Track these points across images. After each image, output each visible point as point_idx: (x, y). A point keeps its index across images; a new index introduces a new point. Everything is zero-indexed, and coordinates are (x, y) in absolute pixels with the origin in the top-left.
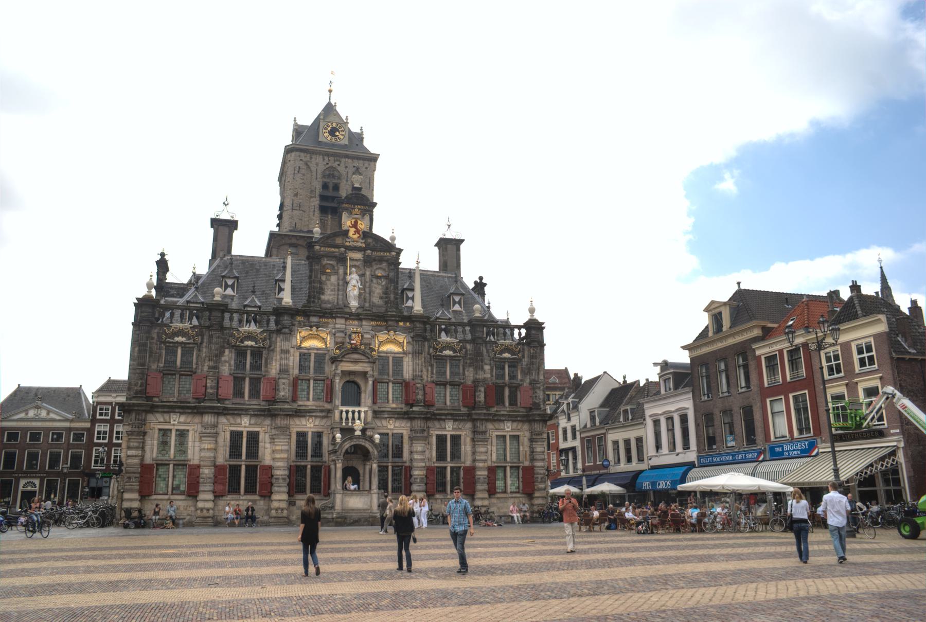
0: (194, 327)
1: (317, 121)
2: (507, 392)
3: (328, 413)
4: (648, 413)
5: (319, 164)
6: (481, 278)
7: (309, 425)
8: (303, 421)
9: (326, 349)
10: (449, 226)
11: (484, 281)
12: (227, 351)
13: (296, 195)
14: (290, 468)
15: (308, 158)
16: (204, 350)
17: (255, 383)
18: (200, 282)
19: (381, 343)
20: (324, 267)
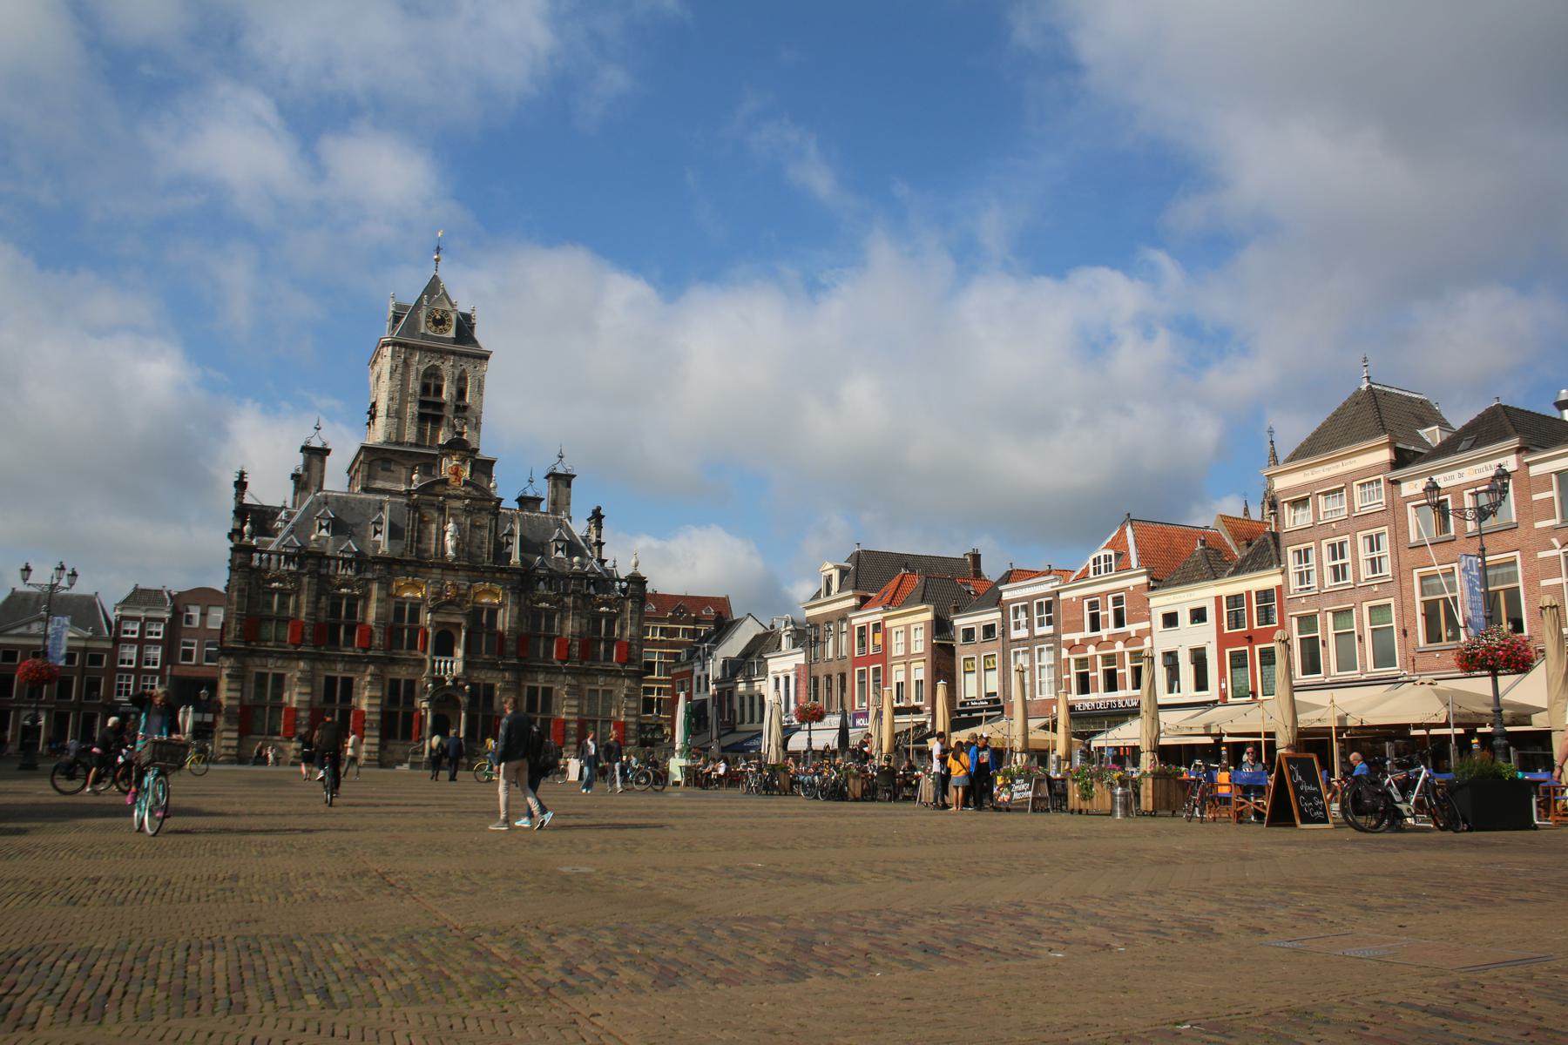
0: (291, 573)
1: (419, 303)
2: (602, 647)
3: (422, 662)
4: (771, 669)
5: (419, 363)
6: (599, 509)
7: (402, 673)
8: (397, 669)
9: (424, 599)
12: (323, 599)
13: (391, 399)
14: (382, 713)
16: (304, 599)
17: (350, 631)
18: (294, 520)
19: (476, 594)
20: (422, 516)
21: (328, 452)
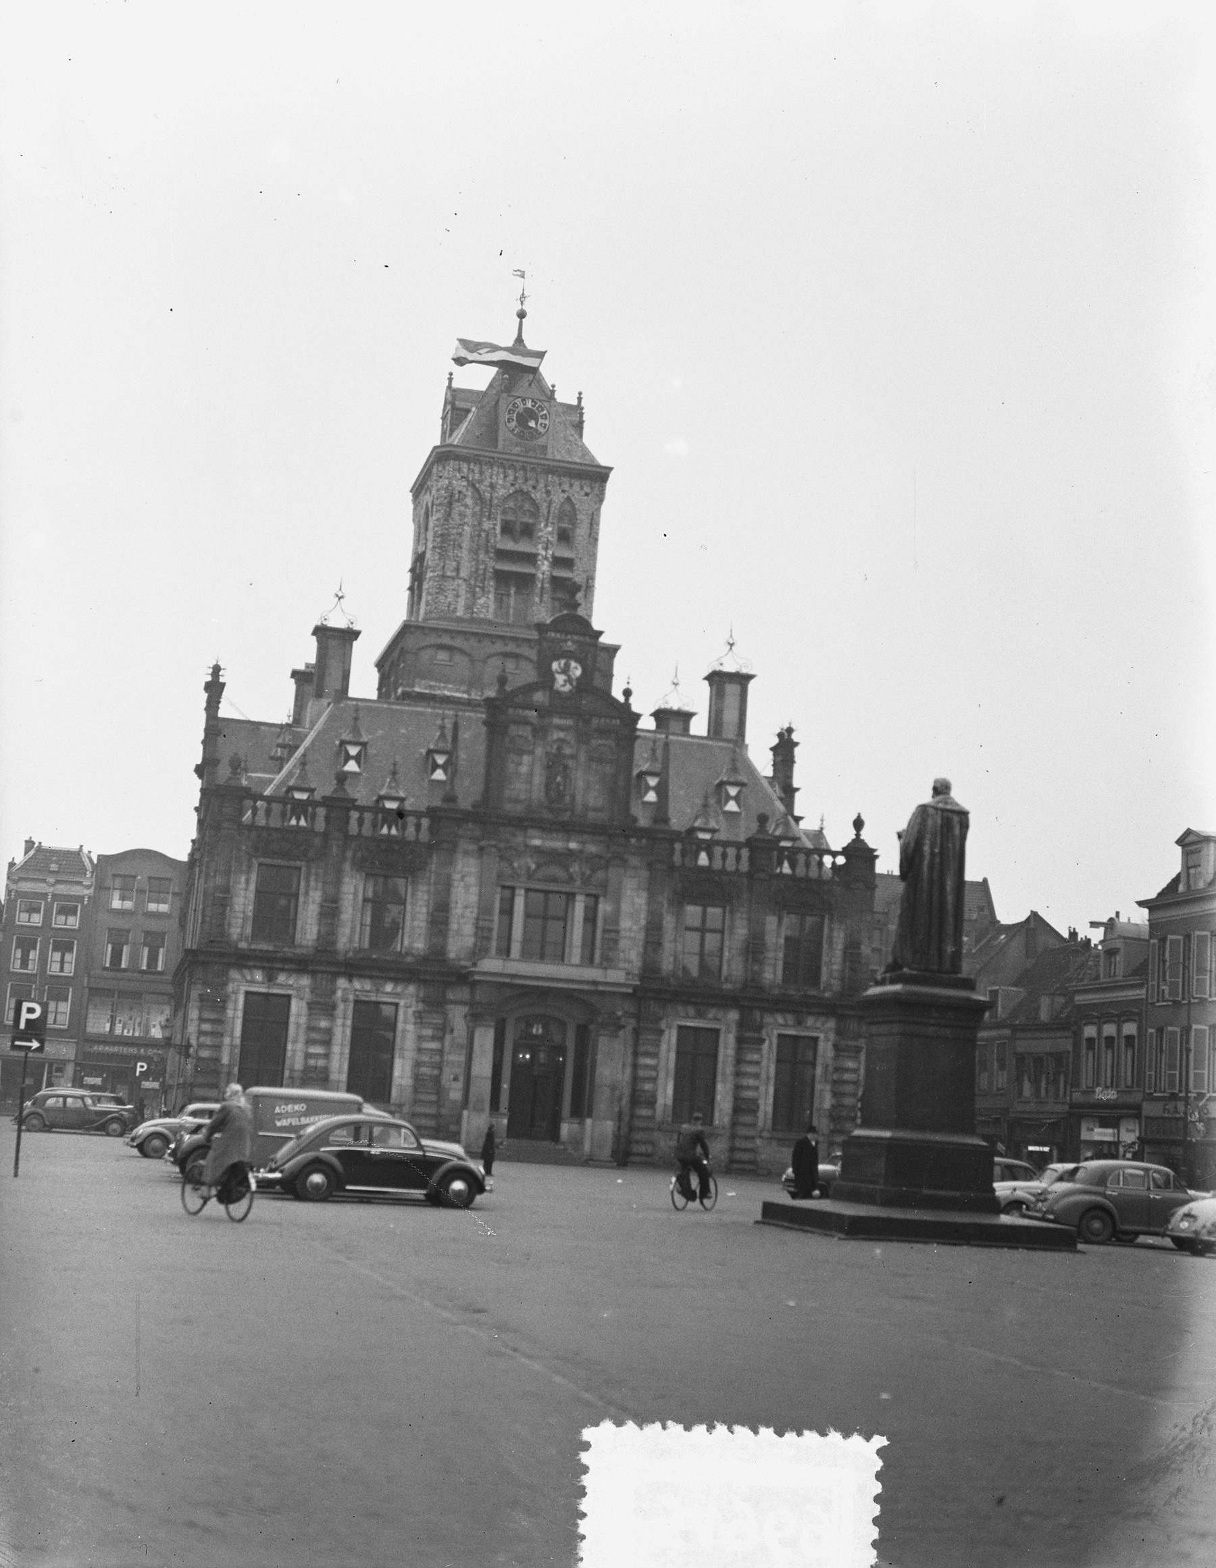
6: (790, 730)
10: (732, 645)
11: (795, 737)
15: (477, 477)
21: (355, 634)
